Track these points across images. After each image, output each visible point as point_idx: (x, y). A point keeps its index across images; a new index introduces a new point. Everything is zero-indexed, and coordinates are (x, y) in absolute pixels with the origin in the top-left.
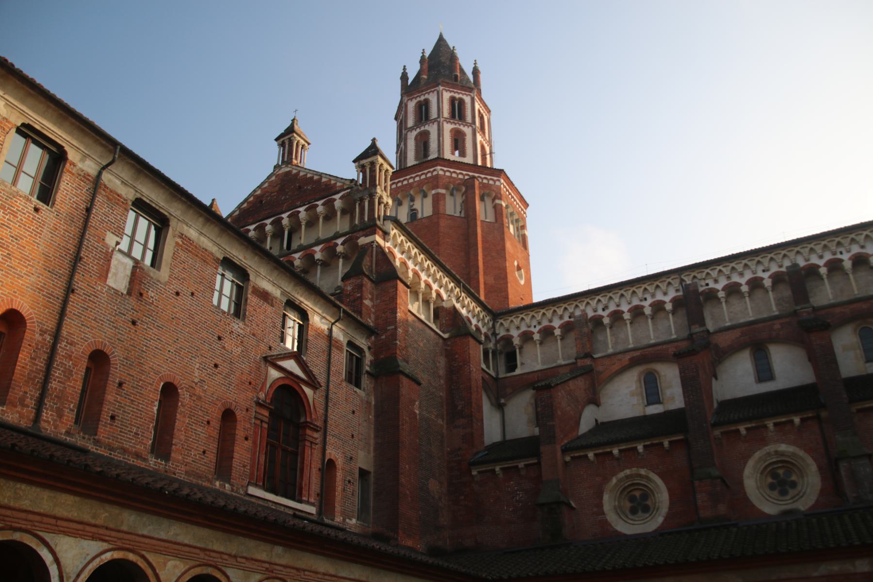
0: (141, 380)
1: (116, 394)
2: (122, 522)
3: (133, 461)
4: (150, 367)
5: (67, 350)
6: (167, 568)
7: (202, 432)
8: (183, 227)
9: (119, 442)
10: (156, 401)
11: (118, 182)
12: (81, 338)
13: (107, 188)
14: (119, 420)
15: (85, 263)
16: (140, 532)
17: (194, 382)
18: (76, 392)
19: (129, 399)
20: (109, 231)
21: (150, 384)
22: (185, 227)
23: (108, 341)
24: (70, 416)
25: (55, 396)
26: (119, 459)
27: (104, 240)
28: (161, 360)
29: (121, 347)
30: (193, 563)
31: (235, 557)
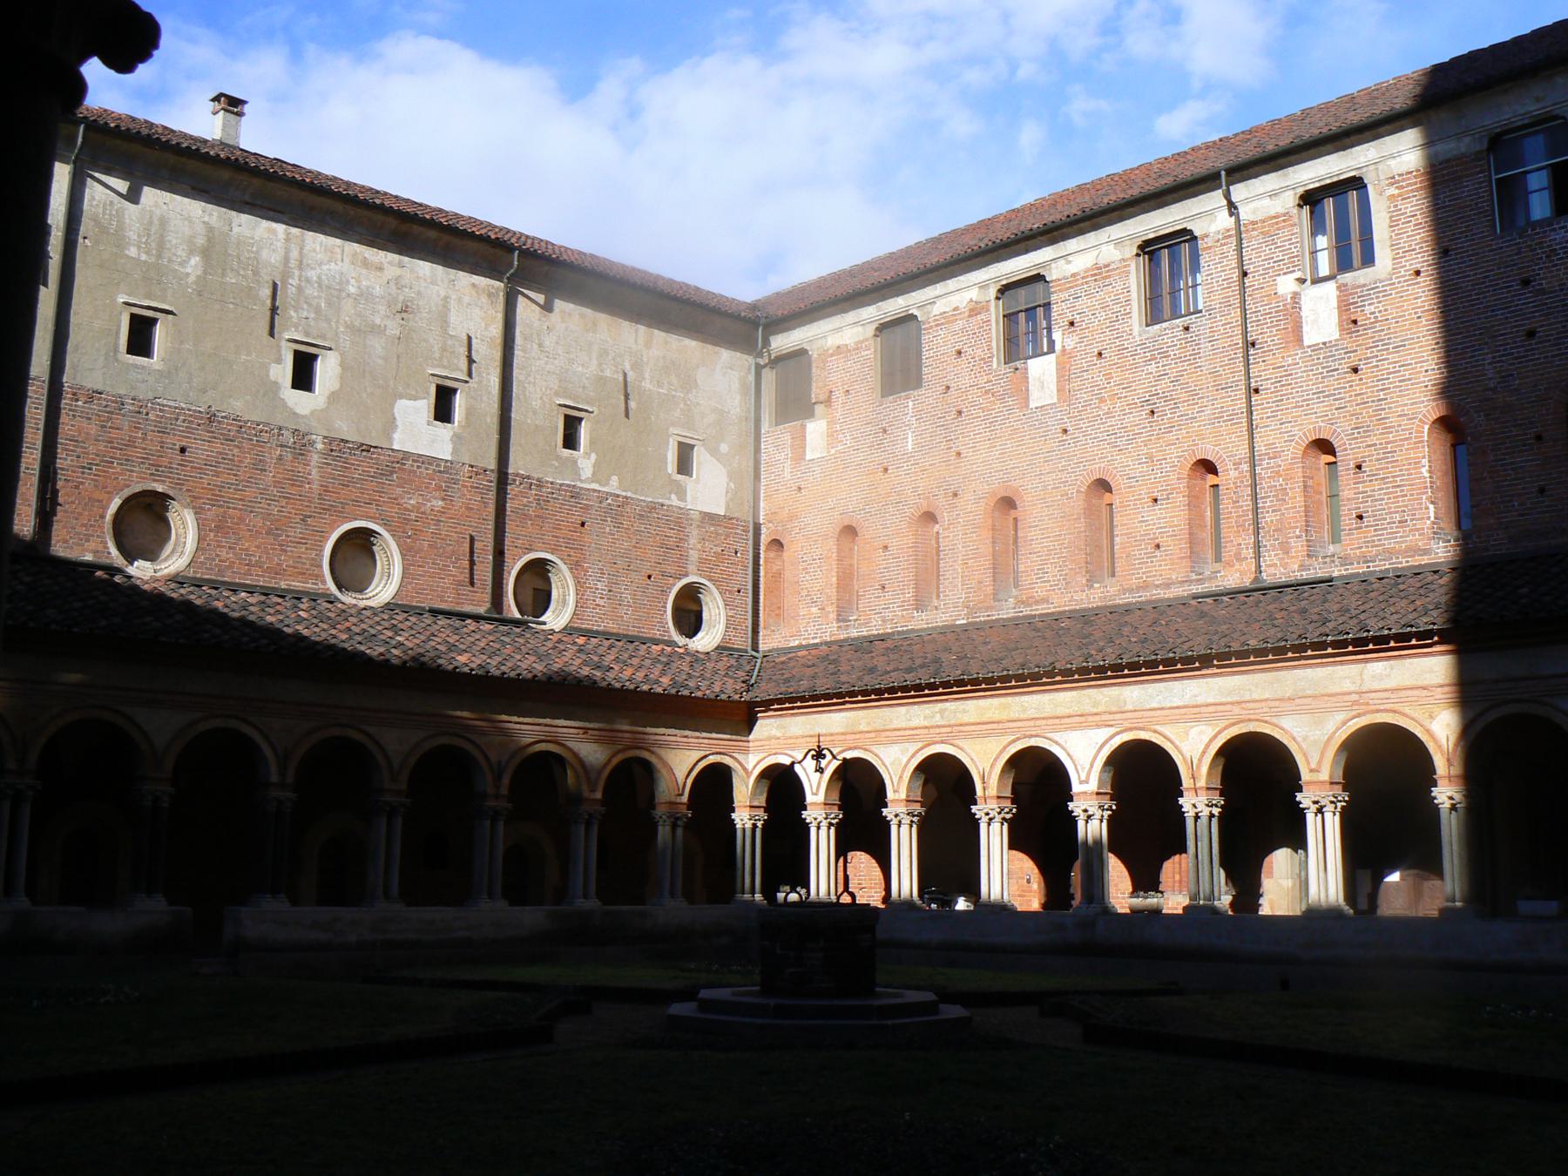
0: (1387, 443)
1: (1355, 483)
2: (1125, 703)
3: (1407, 562)
4: (1399, 416)
5: (1273, 467)
6: (1190, 737)
7: (1527, 461)
8: (1389, 166)
9: (1376, 546)
10: (1424, 457)
11: (1266, 202)
12: (1285, 441)
13: (1256, 223)
14: (1369, 517)
15: (1261, 343)
16: (1148, 707)
17: (1491, 389)
18: (1299, 512)
19: (1376, 480)
20: (1279, 275)
21: (1407, 439)
22: (1392, 163)
23: (1322, 421)
24: (1298, 547)
25: (1274, 531)
26: (1383, 568)
27: (1275, 294)
28: (1415, 393)
29: (1344, 417)
30: (1222, 724)
31: (1289, 699)
